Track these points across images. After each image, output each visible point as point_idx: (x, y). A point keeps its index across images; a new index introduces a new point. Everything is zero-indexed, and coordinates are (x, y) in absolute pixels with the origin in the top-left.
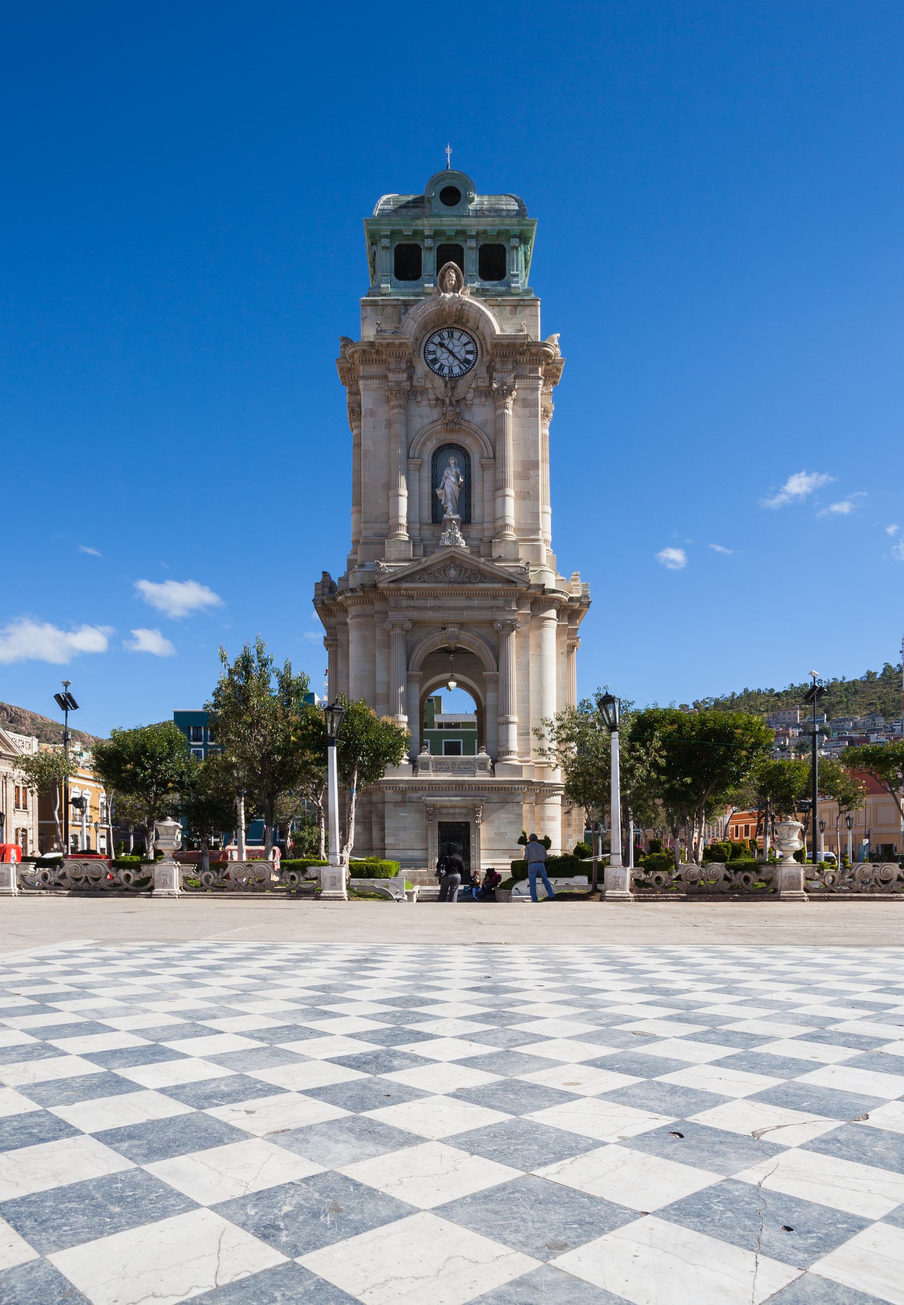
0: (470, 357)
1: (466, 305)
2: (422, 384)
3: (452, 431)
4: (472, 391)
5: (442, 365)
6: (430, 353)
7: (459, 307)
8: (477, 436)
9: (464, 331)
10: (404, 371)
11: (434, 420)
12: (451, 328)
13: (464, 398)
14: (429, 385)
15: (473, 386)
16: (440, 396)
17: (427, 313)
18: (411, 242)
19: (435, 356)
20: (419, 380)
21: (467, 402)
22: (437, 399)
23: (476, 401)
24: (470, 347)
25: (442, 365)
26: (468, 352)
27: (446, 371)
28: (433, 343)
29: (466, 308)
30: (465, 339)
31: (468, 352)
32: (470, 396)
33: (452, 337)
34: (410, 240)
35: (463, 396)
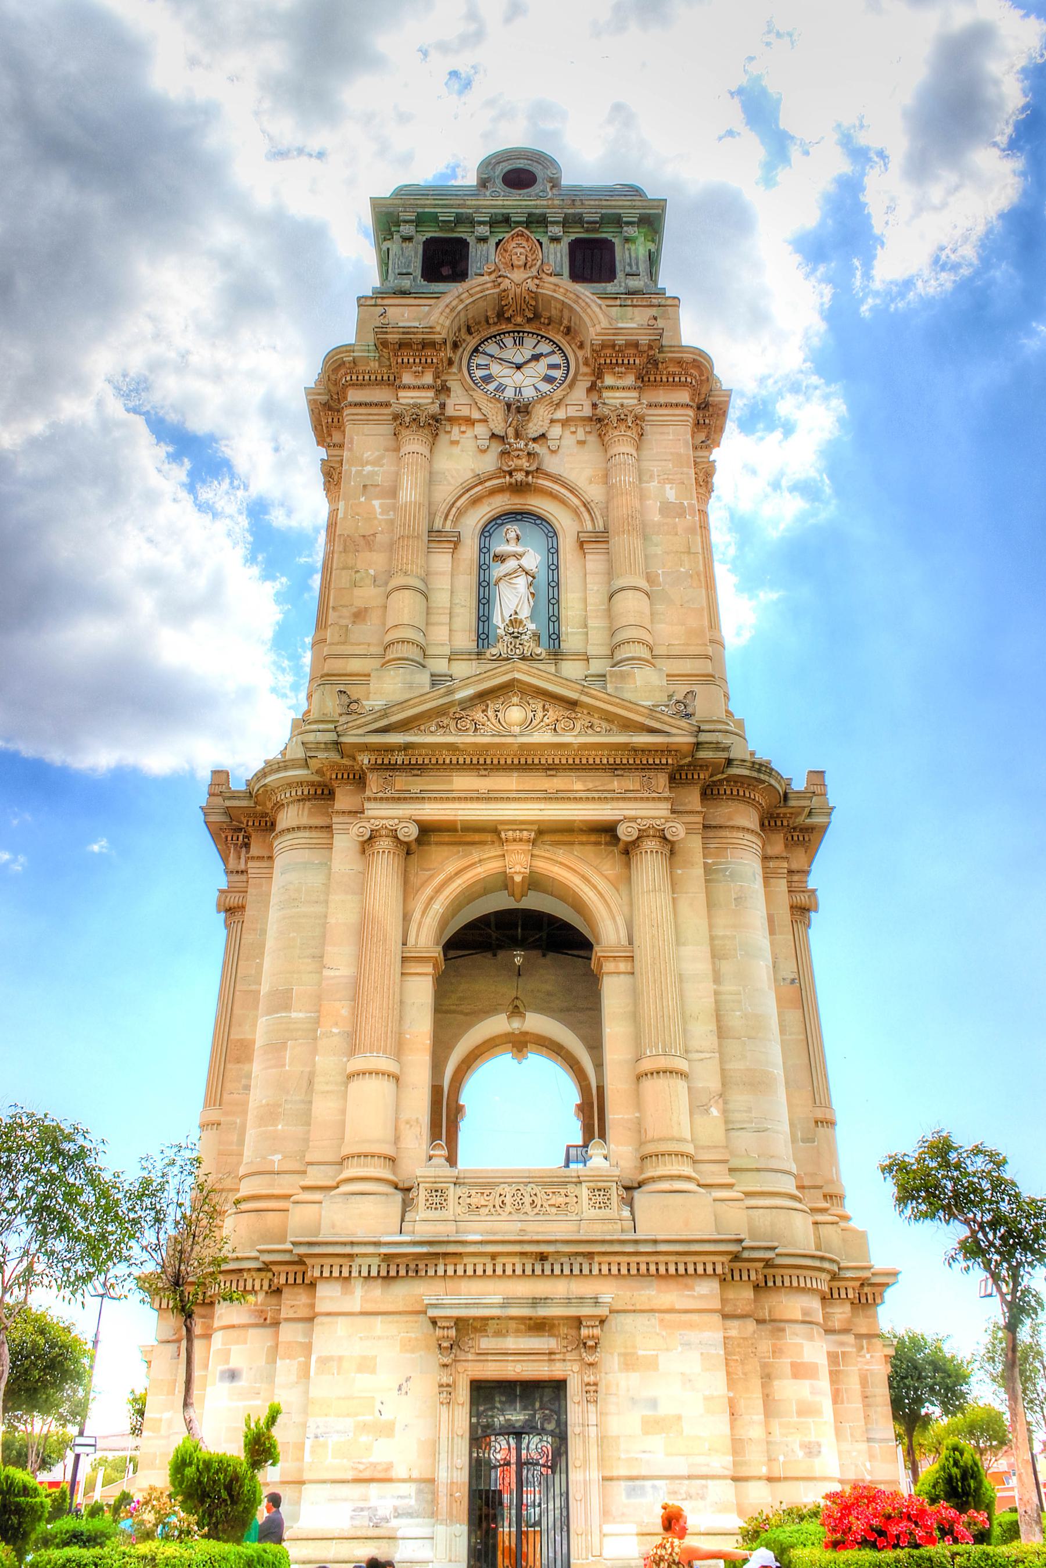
0: (557, 374)
2: (465, 412)
3: (519, 489)
9: (542, 337)
10: (429, 387)
12: (519, 332)
13: (543, 436)
14: (476, 415)
16: (499, 430)
19: (487, 372)
20: (457, 407)
21: (550, 443)
22: (493, 436)
23: (569, 441)
24: (556, 359)
26: (552, 367)
28: (485, 354)
31: (552, 367)
32: (556, 431)
33: (521, 343)
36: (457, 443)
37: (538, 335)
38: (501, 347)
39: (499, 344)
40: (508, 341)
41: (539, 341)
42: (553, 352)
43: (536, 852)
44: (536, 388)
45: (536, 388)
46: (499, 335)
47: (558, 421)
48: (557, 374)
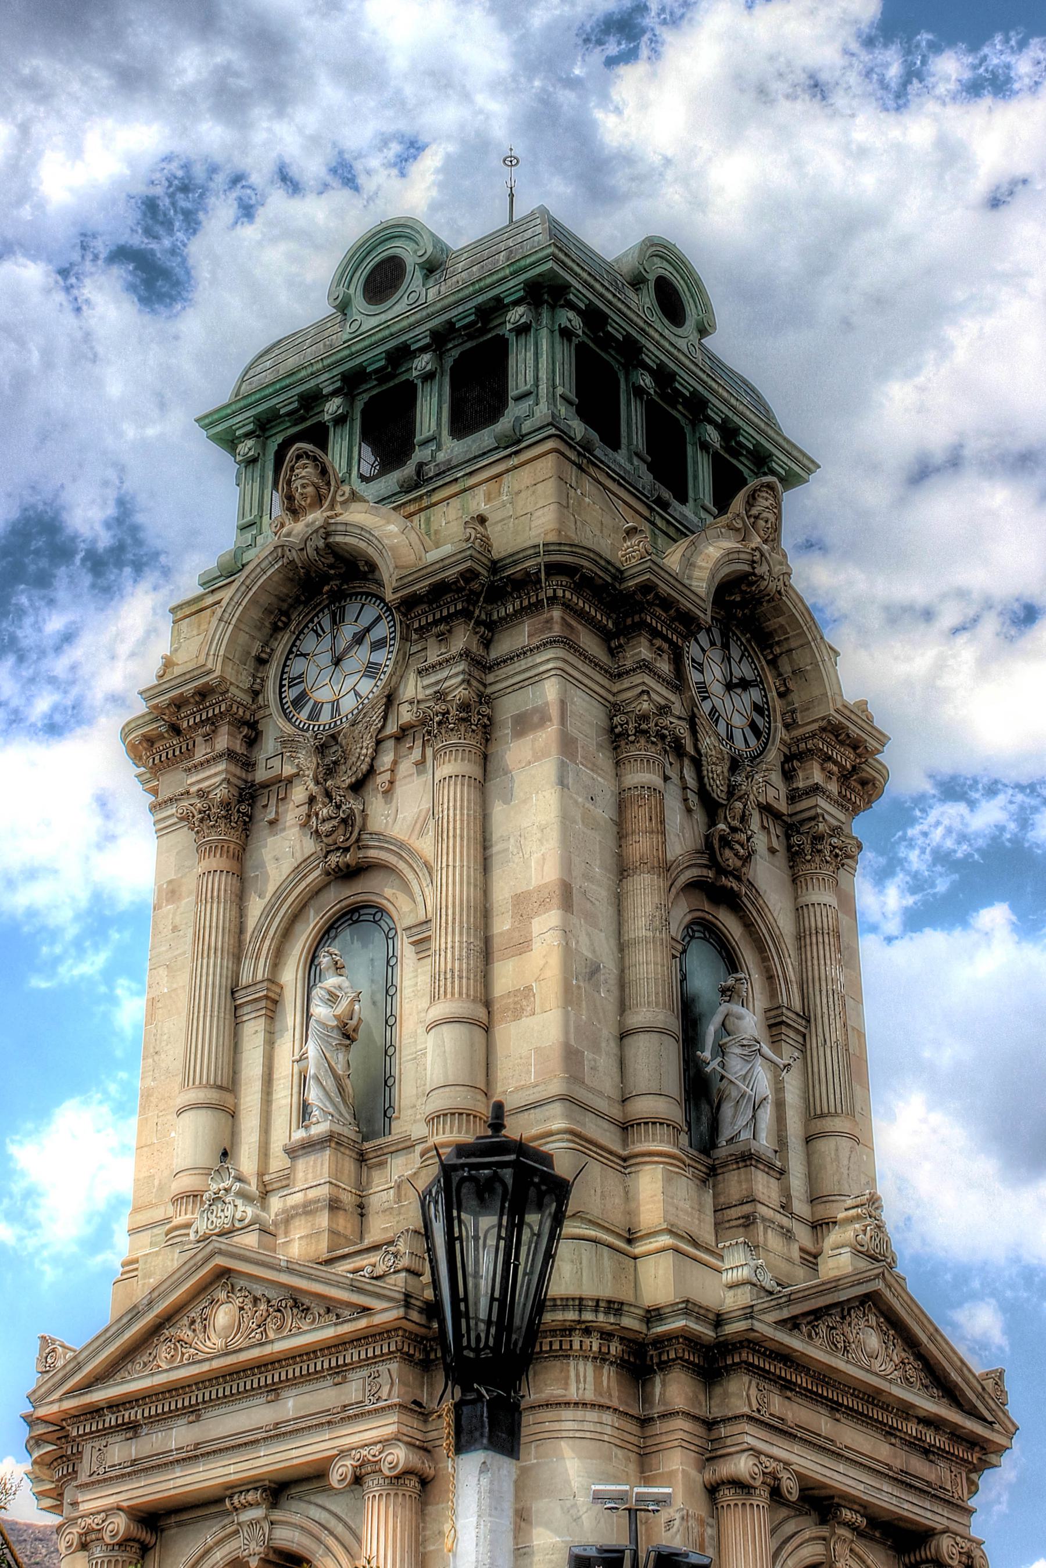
1: (335, 533)
4: (390, 744)
5: (316, 703)
6: (294, 682)
7: (321, 544)
8: (401, 865)
9: (368, 594)
11: (306, 856)
14: (288, 770)
15: (392, 729)
17: (254, 590)
18: (308, 423)
24: (382, 630)
25: (316, 703)
27: (325, 717)
29: (339, 539)
30: (371, 612)
34: (303, 419)
35: (365, 767)
36: (272, 823)
37: (362, 594)
38: (318, 635)
39: (316, 632)
40: (326, 622)
41: (363, 605)
42: (379, 619)
43: (277, 1515)
44: (357, 694)
45: (357, 694)
46: (316, 615)
47: (390, 737)
48: (380, 657)
